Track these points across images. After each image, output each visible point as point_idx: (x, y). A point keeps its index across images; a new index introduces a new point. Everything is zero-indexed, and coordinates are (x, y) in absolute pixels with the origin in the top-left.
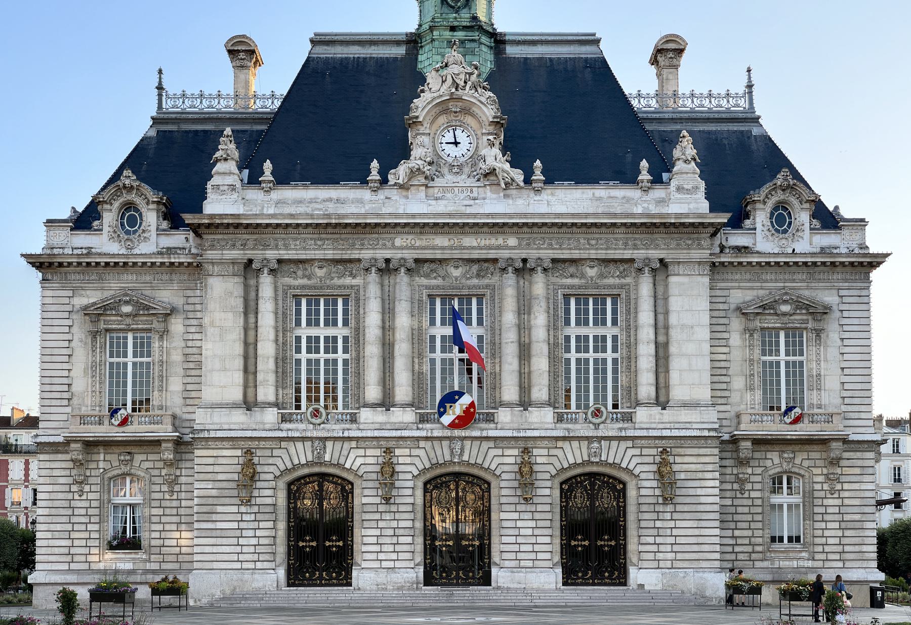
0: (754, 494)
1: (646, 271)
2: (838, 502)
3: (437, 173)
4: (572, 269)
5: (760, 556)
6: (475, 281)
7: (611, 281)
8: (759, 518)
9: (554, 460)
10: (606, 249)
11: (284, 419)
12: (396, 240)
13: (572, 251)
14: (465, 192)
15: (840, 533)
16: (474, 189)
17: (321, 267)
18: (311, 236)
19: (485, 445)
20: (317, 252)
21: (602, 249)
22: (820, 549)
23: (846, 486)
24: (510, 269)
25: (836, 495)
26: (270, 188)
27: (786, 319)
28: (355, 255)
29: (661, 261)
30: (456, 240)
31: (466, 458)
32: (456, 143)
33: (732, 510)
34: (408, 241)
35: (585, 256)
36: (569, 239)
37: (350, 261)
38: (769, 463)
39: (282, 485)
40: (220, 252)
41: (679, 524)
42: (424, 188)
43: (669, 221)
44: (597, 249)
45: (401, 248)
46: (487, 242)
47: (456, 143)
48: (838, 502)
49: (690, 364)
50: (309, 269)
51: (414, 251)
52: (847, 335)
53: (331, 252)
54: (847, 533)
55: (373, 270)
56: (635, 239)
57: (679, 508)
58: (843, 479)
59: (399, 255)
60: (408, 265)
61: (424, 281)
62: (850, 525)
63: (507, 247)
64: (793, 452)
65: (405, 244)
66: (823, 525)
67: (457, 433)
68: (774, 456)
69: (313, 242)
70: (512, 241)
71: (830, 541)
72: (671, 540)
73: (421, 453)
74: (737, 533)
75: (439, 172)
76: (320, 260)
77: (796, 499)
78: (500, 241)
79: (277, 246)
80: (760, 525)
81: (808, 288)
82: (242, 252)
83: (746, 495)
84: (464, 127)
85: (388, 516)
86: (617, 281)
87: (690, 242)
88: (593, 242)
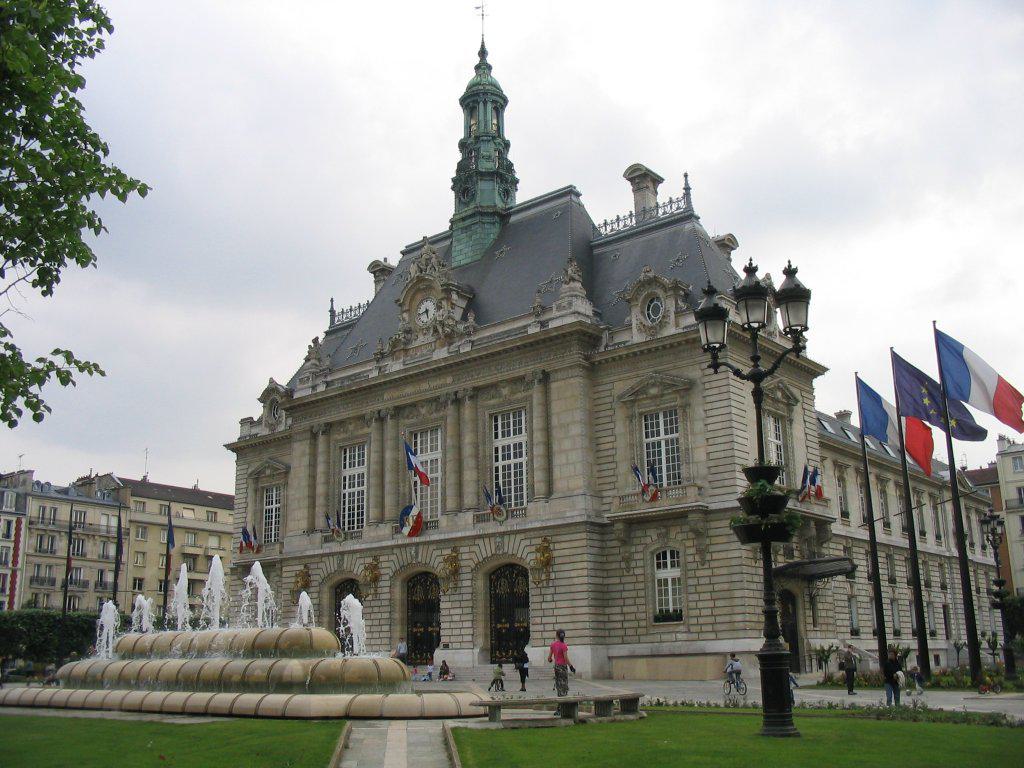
0: (637, 571)
2: (709, 572)
4: (493, 392)
5: (644, 631)
6: (435, 415)
7: (519, 396)
8: (642, 593)
9: (473, 556)
11: (327, 540)
15: (711, 604)
17: (350, 424)
19: (431, 548)
22: (694, 621)
23: (715, 556)
25: (706, 566)
27: (658, 401)
31: (419, 559)
32: (427, 311)
33: (621, 587)
38: (649, 540)
39: (326, 589)
41: (559, 604)
47: (427, 311)
48: (708, 572)
49: (567, 459)
52: (709, 406)
54: (718, 603)
57: (558, 590)
58: (712, 548)
61: (407, 421)
62: (720, 595)
63: (446, 385)
64: (665, 527)
66: (696, 597)
67: (416, 540)
68: (653, 534)
70: (449, 380)
71: (704, 612)
72: (553, 620)
73: (393, 557)
74: (625, 609)
77: (675, 573)
80: (643, 601)
81: (675, 368)
83: (631, 573)
85: (376, 610)
86: (524, 394)
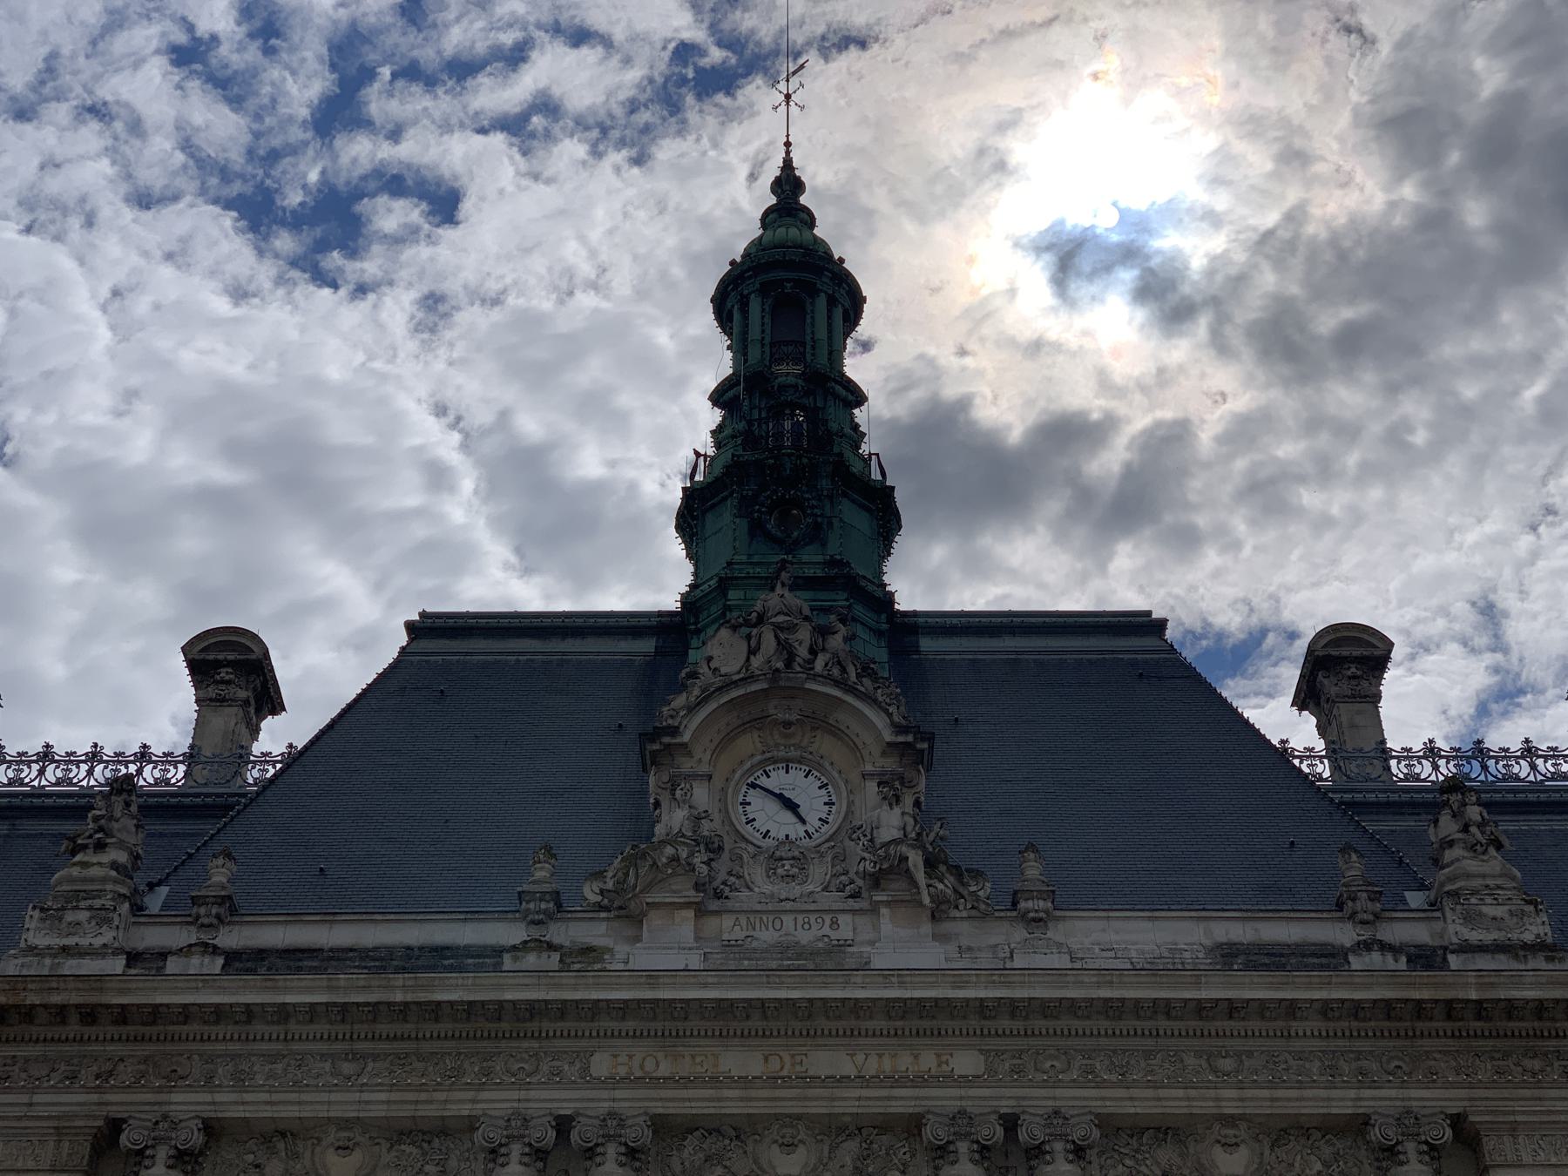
1: (1412, 1155)
3: (733, 879)
10: (1271, 1085)
12: (596, 1057)
13: (1162, 1093)
14: (815, 927)
16: (844, 919)
17: (344, 1149)
18: (323, 1047)
20: (334, 1097)
21: (1256, 1085)
24: (963, 1147)
26: (218, 916)
28: (460, 1104)
29: (1457, 1122)
30: (787, 1059)
34: (636, 1062)
35: (1207, 1108)
36: (1148, 1054)
37: (443, 1130)
40: (24, 1099)
42: (690, 914)
43: (1461, 995)
44: (1240, 1086)
45: (613, 1082)
46: (887, 1065)
50: (308, 1154)
51: (653, 1093)
53: (383, 1096)
55: (516, 1149)
56: (1359, 1055)
59: (598, 1103)
60: (630, 1135)
63: (949, 1079)
65: (622, 1071)
69: (327, 1066)
70: (966, 1062)
75: (739, 877)
76: (345, 1124)
78: (928, 1061)
79: (210, 1078)
82: (94, 1097)
84: (812, 764)
87: (1536, 1064)
88: (1227, 1064)
